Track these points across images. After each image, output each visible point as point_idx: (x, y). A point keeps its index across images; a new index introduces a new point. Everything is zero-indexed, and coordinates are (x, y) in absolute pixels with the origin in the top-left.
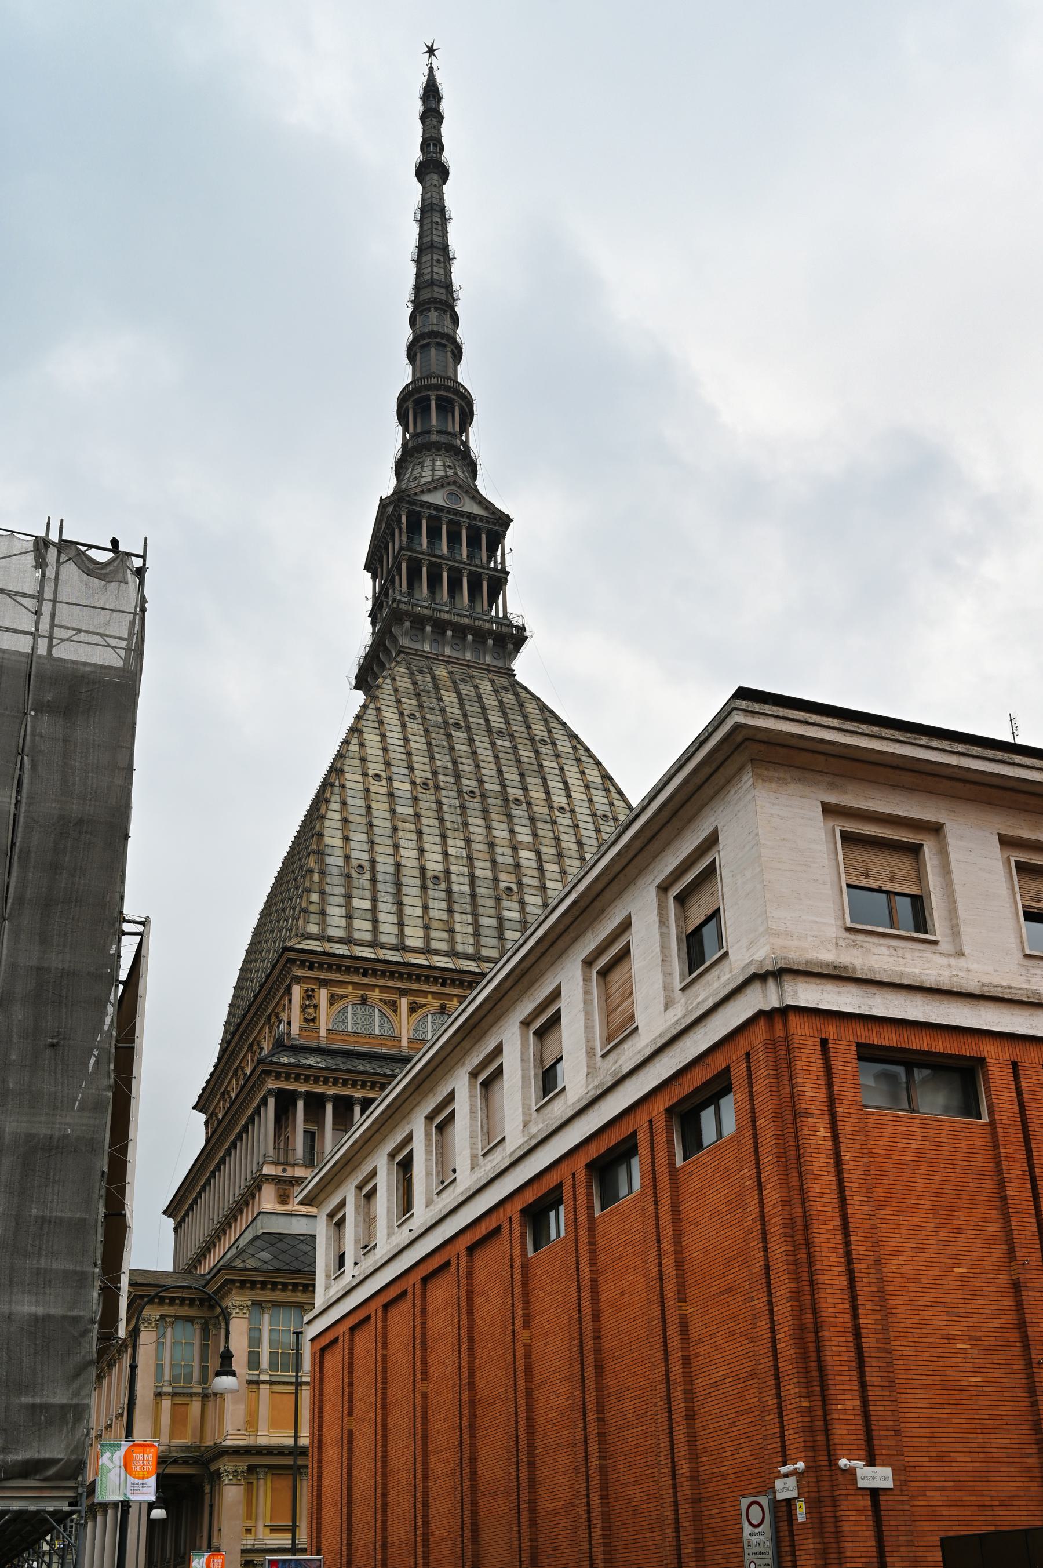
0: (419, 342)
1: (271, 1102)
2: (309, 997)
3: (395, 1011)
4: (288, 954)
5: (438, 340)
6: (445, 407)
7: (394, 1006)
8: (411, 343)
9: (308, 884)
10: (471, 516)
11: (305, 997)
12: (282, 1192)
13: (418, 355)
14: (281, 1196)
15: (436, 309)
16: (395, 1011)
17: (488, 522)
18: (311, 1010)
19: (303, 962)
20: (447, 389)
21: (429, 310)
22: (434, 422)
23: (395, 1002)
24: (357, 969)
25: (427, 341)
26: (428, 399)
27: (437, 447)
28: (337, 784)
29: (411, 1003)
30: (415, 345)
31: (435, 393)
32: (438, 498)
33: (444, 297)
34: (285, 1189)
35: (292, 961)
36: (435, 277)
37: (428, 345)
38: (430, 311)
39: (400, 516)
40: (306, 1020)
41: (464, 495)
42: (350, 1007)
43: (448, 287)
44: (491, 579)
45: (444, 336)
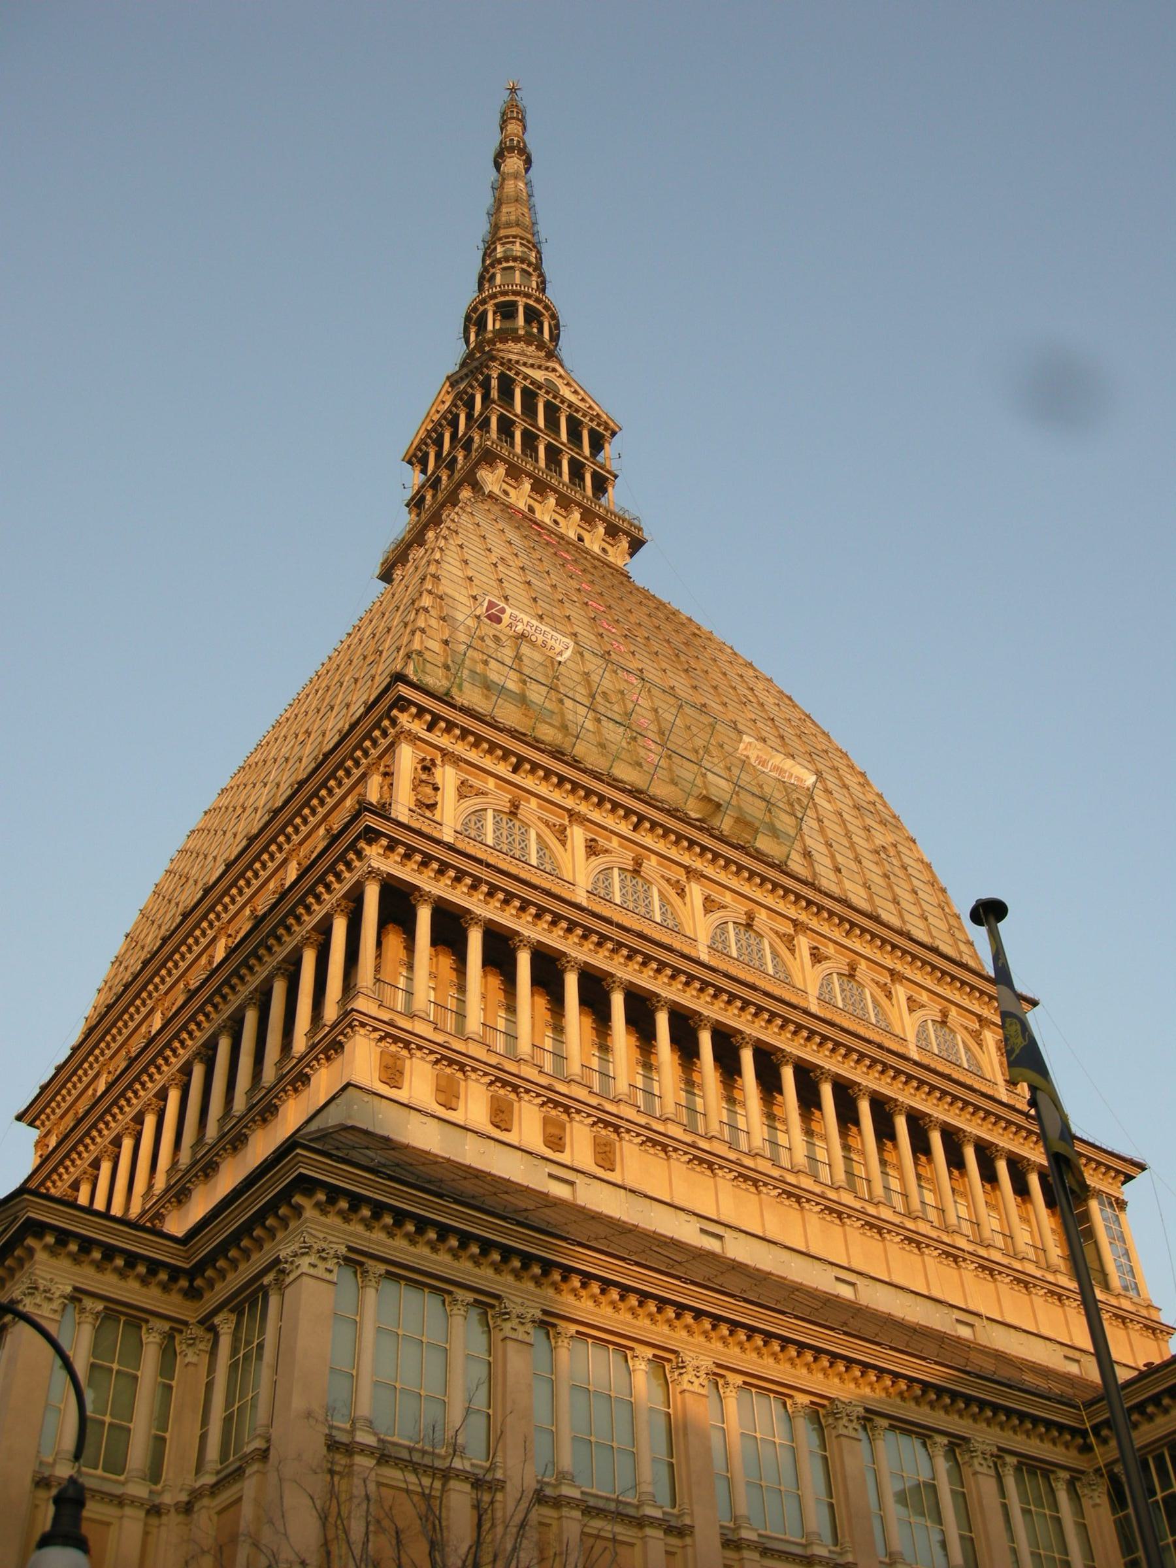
1: (372, 895)
2: (425, 769)
3: (563, 843)
4: (404, 690)
5: (525, 266)
7: (561, 835)
9: (421, 623)
10: (570, 405)
11: (419, 766)
12: (390, 1061)
13: (498, 277)
14: (387, 1067)
16: (563, 843)
17: (591, 420)
18: (428, 790)
19: (422, 711)
20: (538, 301)
21: (515, 242)
23: (563, 829)
24: (507, 754)
25: (511, 264)
26: (514, 304)
28: (451, 541)
29: (586, 840)
31: (524, 299)
32: (539, 376)
34: (395, 1056)
35: (402, 703)
37: (512, 268)
39: (488, 378)
40: (420, 803)
41: (565, 387)
42: (490, 813)
44: (595, 475)
45: (530, 264)
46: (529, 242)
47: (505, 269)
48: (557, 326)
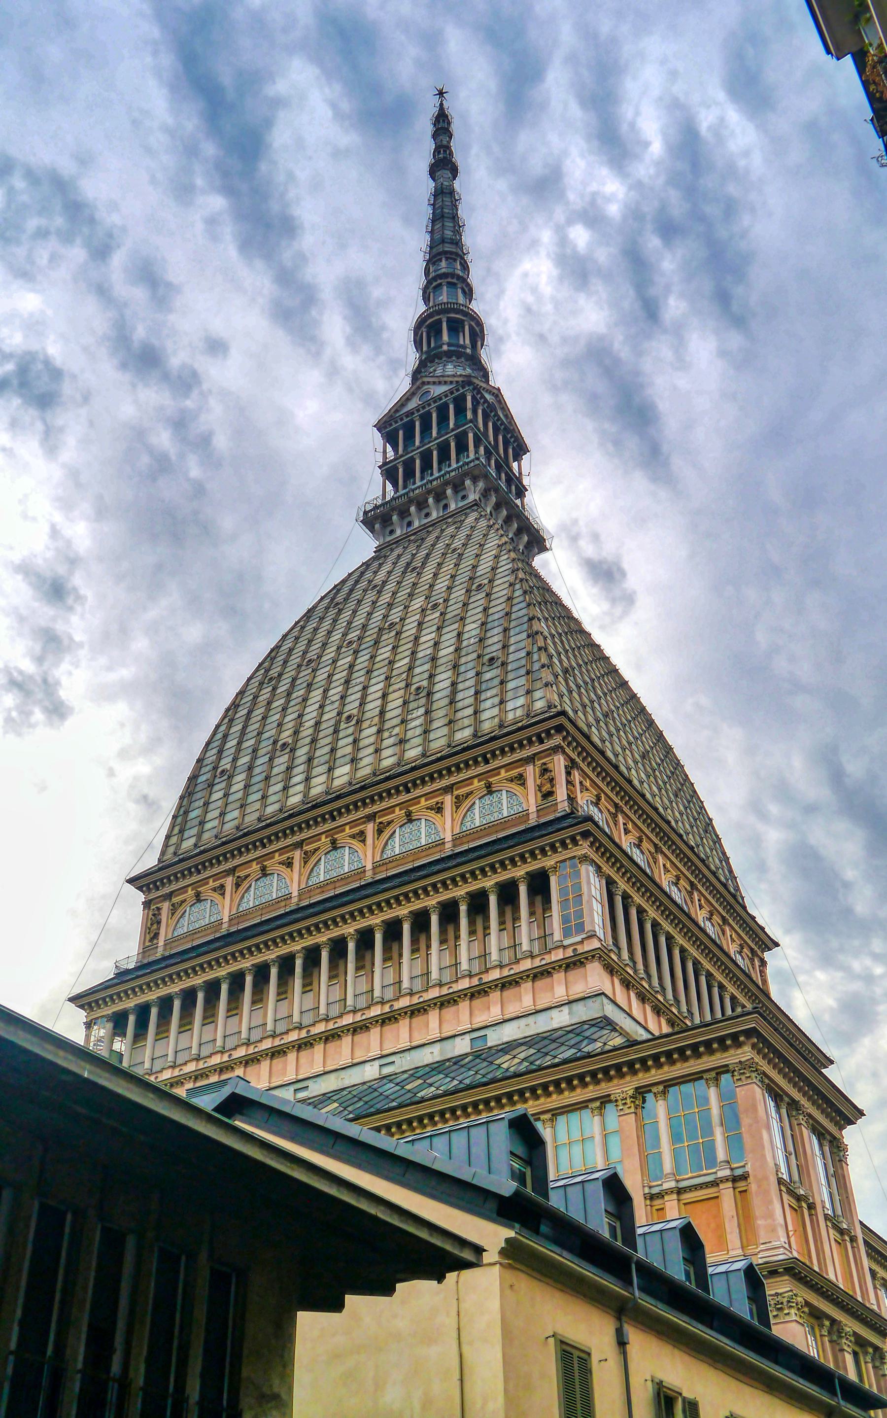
0: (432, 284)
5: (449, 280)
6: (455, 327)
8: (426, 286)
13: (432, 295)
15: (447, 259)
21: (441, 260)
22: (445, 337)
25: (439, 281)
26: (439, 322)
27: (449, 354)
30: (428, 288)
33: (454, 250)
36: (446, 236)
37: (440, 284)
38: (441, 261)
43: (458, 243)
46: (451, 253)
47: (435, 288)
48: (480, 324)
